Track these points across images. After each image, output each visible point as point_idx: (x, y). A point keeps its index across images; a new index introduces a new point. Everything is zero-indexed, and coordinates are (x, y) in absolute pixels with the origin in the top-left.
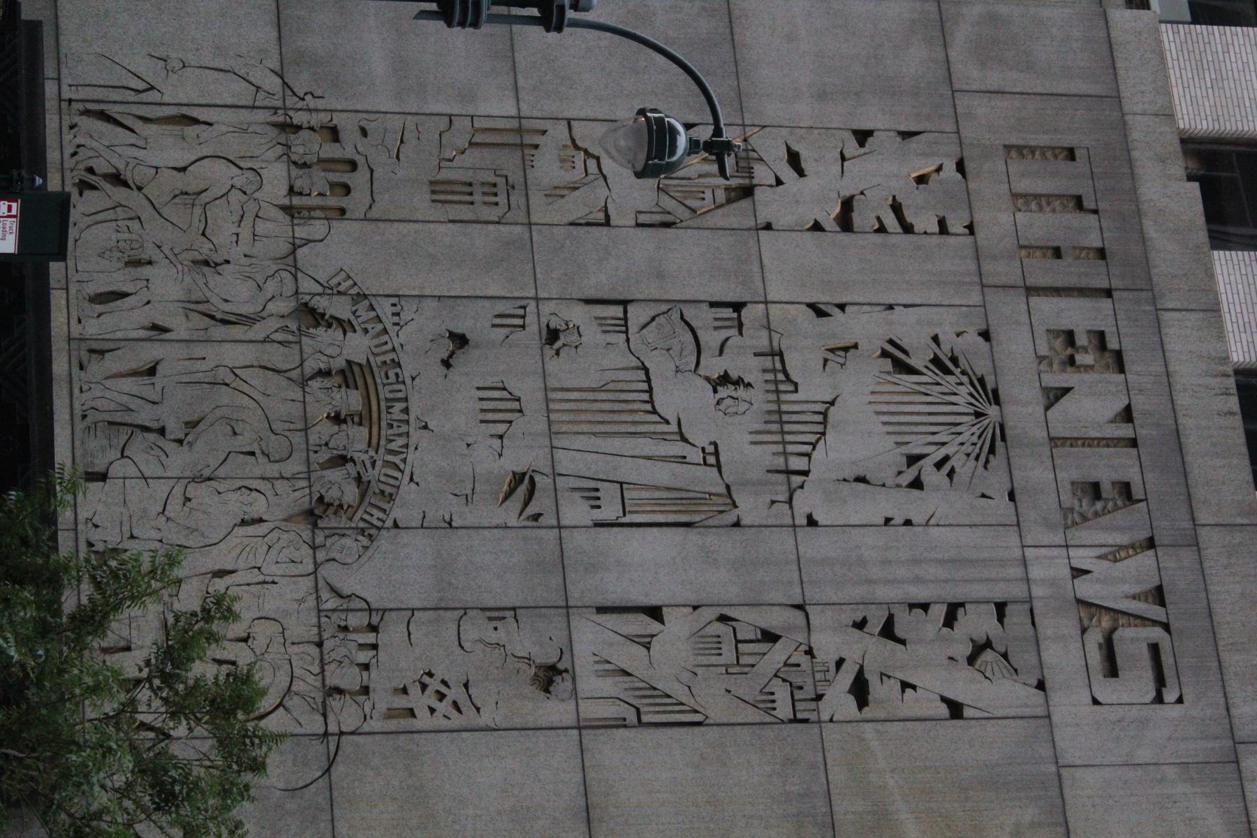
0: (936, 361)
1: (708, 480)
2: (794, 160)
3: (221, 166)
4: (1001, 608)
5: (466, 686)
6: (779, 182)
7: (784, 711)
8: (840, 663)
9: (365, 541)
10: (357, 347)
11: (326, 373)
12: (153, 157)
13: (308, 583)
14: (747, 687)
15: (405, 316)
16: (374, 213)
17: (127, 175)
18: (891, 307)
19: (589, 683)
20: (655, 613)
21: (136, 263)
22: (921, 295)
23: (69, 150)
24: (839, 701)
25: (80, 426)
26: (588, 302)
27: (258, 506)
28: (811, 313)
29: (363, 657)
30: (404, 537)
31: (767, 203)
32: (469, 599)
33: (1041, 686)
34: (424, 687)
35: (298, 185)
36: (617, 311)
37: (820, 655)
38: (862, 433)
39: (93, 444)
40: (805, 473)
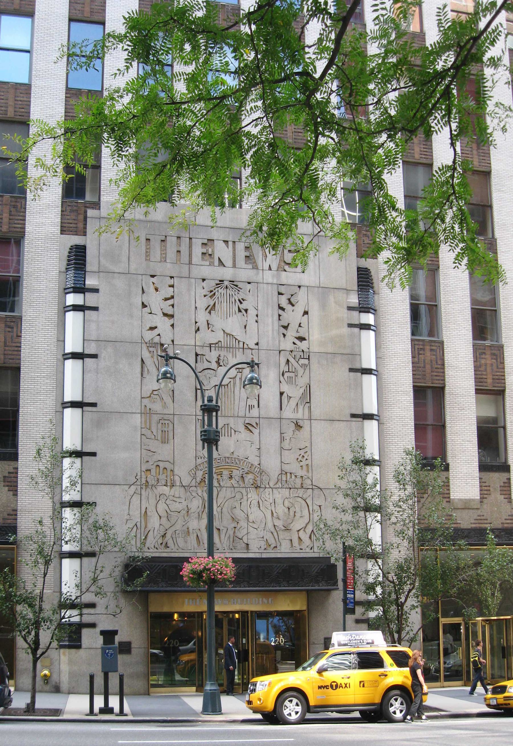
0: (211, 297)
2: (152, 329)
3: (159, 506)
4: (280, 294)
6: (159, 335)
7: (306, 362)
8: (294, 343)
9: (263, 473)
12: (157, 525)
13: (274, 490)
14: (301, 371)
15: (202, 456)
16: (172, 461)
17: (162, 534)
18: (196, 307)
19: (300, 415)
20: (282, 394)
21: (188, 532)
22: (192, 298)
23: (156, 550)
24: (303, 345)
25: (234, 551)
26: (196, 400)
27: (255, 502)
28: (198, 332)
29: (293, 477)
30: (262, 462)
33: (299, 287)
34: (301, 461)
35: (164, 483)
37: (292, 349)
38: (233, 324)
39: (239, 547)
40: (244, 343)
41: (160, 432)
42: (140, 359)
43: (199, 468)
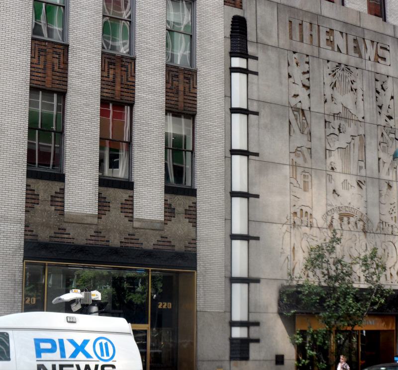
1: (357, 139)
5: (391, 204)
6: (300, 102)
8: (386, 121)
10: (336, 216)
11: (341, 225)
13: (376, 235)
16: (310, 206)
18: (324, 83)
24: (391, 122)
26: (326, 158)
31: (305, 107)
32: (378, 200)
33: (388, 76)
34: (392, 214)
36: (327, 151)
41: (303, 182)
42: (288, 120)
43: (329, 214)
